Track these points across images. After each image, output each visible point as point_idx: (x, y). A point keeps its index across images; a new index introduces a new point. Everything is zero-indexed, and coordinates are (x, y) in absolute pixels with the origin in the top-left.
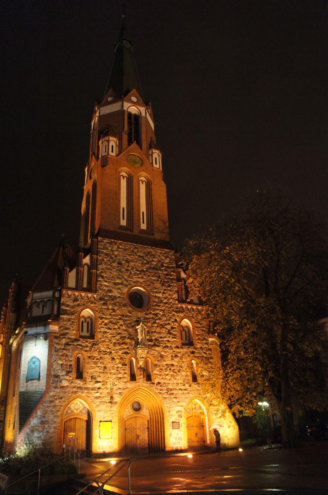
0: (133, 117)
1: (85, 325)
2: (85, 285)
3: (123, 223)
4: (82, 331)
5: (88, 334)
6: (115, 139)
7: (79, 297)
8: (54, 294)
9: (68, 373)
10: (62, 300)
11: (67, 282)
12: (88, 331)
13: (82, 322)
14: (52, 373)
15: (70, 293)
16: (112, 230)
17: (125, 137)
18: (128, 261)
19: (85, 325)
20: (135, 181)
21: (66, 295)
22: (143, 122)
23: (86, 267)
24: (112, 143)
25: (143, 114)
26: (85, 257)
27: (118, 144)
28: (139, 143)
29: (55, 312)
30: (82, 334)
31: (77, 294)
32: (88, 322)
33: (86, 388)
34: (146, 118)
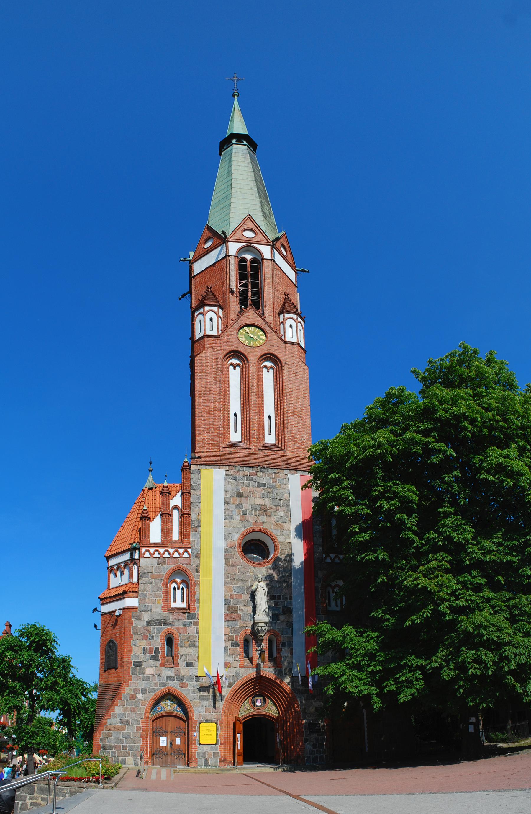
0: (249, 265)
1: (179, 592)
3: (236, 437)
4: (175, 601)
5: (184, 605)
7: (166, 555)
8: (131, 555)
9: (154, 658)
10: (142, 561)
11: (147, 536)
12: (183, 601)
13: (175, 589)
14: (133, 659)
15: (152, 550)
16: (215, 450)
17: (233, 302)
18: (239, 495)
19: (179, 592)
20: (253, 370)
21: (147, 555)
22: (267, 267)
28: (257, 305)
29: (135, 580)
30: (173, 605)
31: (162, 550)
32: (183, 589)
33: (182, 679)
34: (272, 260)
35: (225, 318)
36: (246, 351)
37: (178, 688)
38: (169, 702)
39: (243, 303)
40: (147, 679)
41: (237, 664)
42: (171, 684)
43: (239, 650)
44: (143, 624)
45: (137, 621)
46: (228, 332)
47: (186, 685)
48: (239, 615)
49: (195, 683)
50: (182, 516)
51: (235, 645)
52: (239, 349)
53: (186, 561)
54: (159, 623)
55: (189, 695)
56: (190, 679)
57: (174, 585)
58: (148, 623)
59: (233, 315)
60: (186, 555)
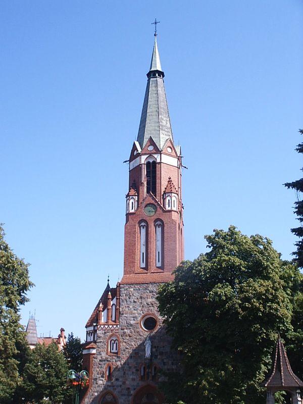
1: (115, 345)
2: (114, 319)
5: (117, 351)
6: (134, 197)
9: (102, 377)
15: (102, 326)
18: (141, 298)
19: (115, 345)
23: (114, 307)
24: (132, 201)
25: (158, 161)
26: (112, 300)
27: (136, 199)
30: (112, 351)
31: (106, 326)
33: (114, 386)
35: (138, 201)
36: (148, 219)
37: (112, 390)
38: (109, 397)
39: (148, 192)
40: (99, 386)
41: (138, 379)
42: (109, 388)
43: (139, 372)
44: (97, 361)
45: (95, 360)
46: (140, 209)
47: (116, 389)
48: (139, 356)
49: (119, 388)
50: (116, 309)
51: (137, 370)
52: (144, 218)
53: (117, 331)
54: (105, 361)
55: (115, 393)
56: (118, 386)
57: (113, 342)
58: (100, 361)
59: (141, 201)
60: (117, 328)
